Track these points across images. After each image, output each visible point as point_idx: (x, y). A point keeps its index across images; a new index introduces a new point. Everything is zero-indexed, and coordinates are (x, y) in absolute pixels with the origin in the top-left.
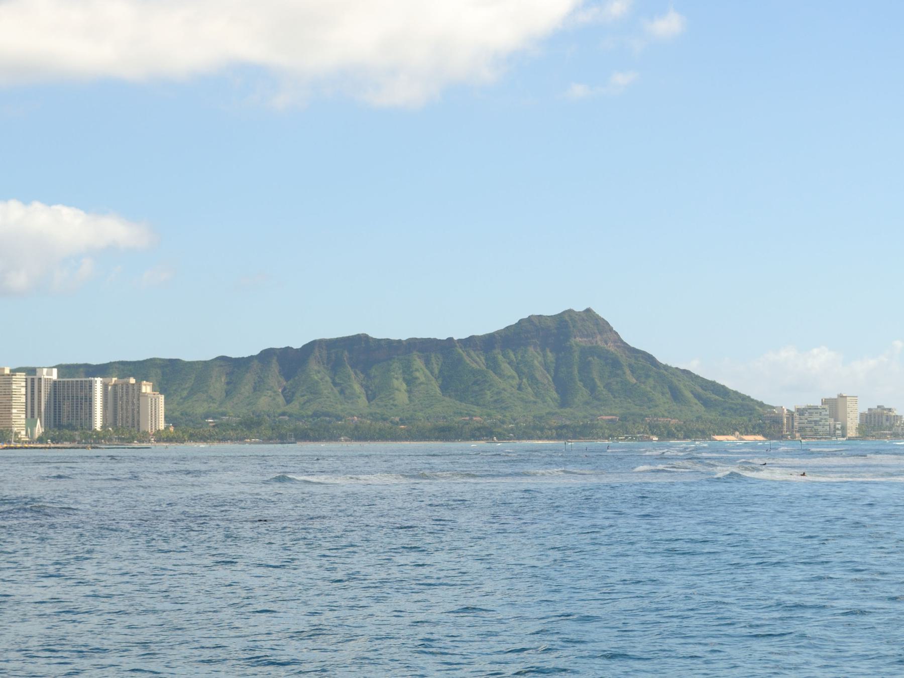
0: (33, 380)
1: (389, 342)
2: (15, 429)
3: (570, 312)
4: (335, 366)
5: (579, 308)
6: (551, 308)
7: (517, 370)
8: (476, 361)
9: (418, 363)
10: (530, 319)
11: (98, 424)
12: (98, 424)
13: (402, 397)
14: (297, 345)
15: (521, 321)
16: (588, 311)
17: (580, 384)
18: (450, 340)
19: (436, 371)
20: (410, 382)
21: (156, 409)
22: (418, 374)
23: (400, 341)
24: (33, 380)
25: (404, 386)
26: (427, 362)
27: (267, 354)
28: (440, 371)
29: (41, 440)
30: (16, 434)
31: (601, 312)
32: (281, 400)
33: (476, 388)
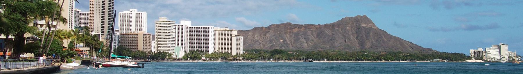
0: (179, 26)
2: (169, 52)
5: (362, 15)
6: (353, 15)
7: (343, 35)
8: (328, 32)
12: (211, 51)
13: (305, 45)
18: (319, 25)
19: (315, 36)
20: (307, 40)
23: (302, 25)
24: (179, 26)
25: (305, 41)
27: (255, 29)
28: (317, 36)
29: (185, 58)
30: (170, 55)
31: (369, 16)
32: (261, 45)
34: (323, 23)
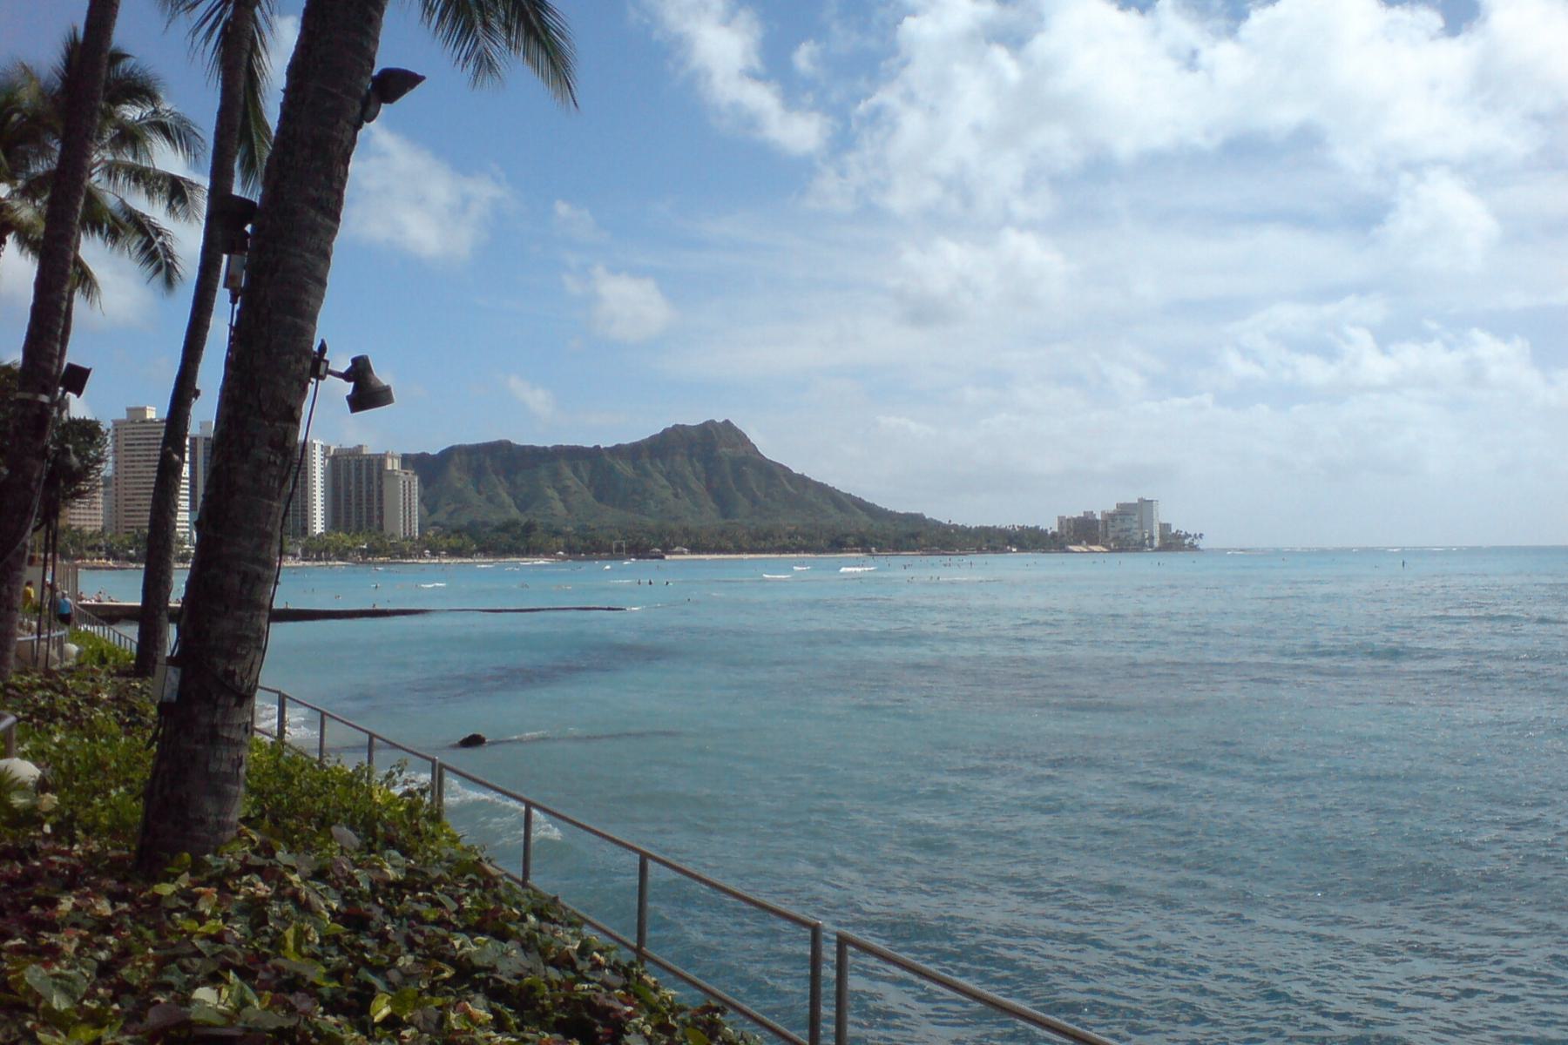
1: (533, 449)
3: (712, 422)
4: (478, 473)
5: (720, 420)
7: (668, 478)
8: (624, 468)
9: (567, 471)
10: (676, 427)
11: (318, 526)
12: (318, 526)
14: (434, 450)
15: (665, 431)
16: (727, 422)
17: (739, 495)
18: (597, 447)
20: (563, 491)
21: (405, 508)
22: (569, 483)
26: (575, 470)
33: (637, 497)
34: (607, 443)
